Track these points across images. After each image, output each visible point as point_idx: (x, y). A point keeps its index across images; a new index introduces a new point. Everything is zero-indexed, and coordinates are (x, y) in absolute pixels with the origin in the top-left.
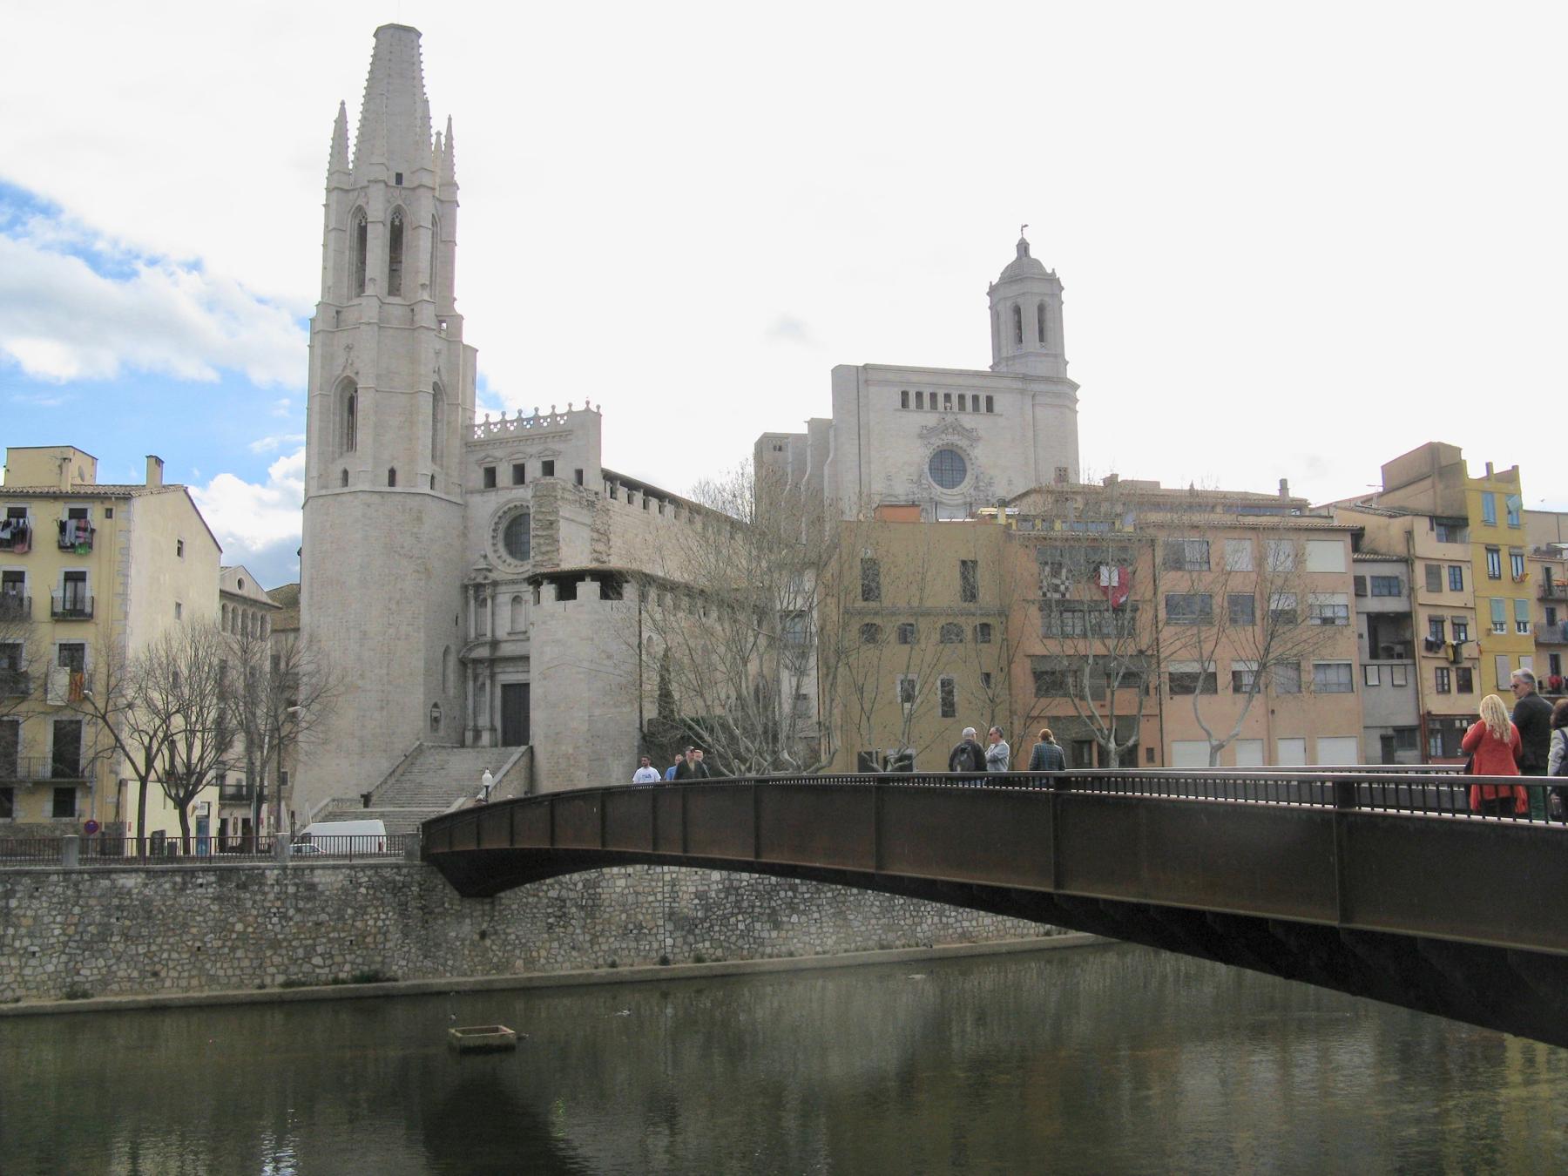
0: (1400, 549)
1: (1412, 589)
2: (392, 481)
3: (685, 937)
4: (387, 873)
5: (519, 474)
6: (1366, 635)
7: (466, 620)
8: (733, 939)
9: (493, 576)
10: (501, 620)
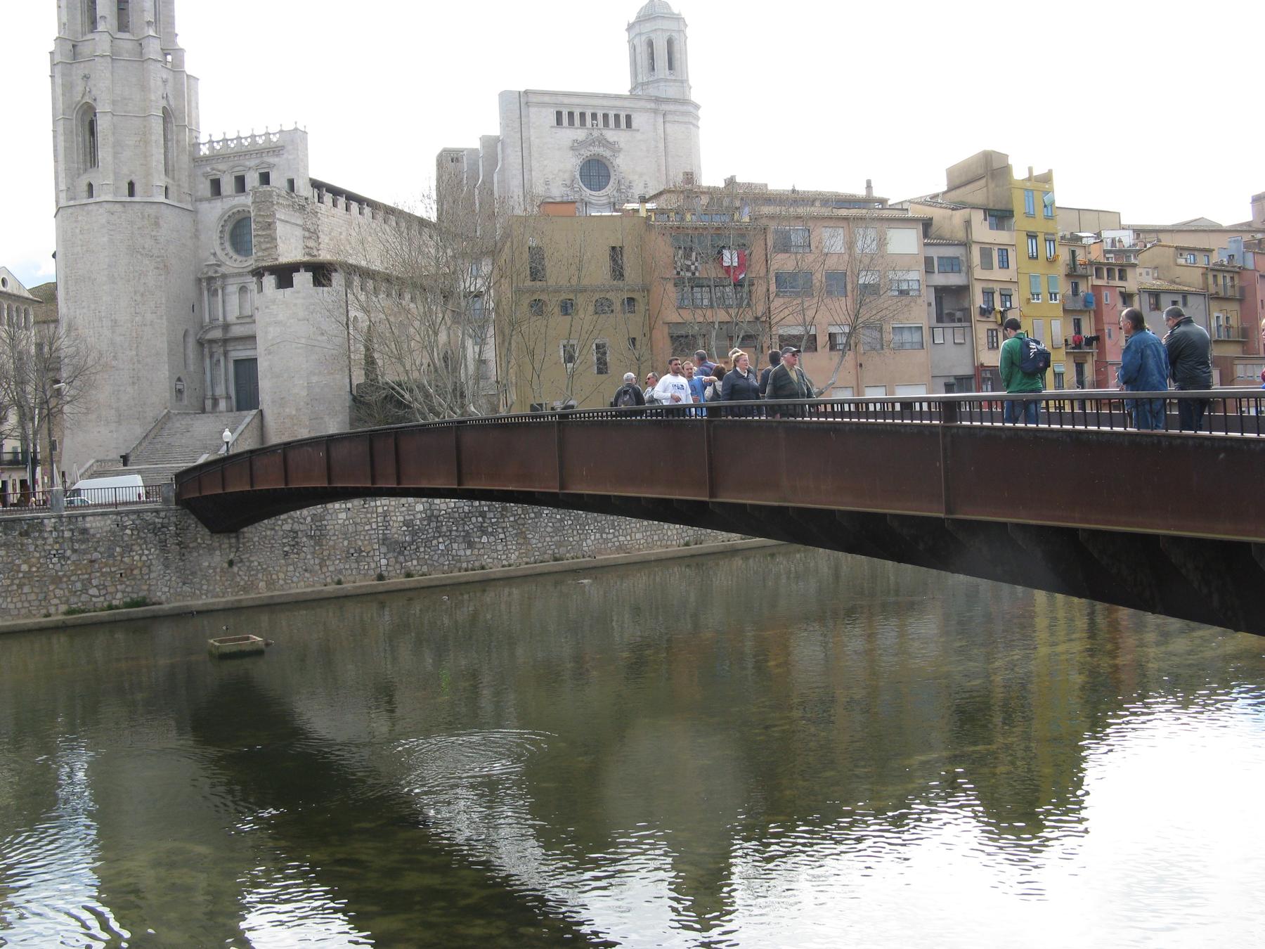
0: (961, 235)
1: (970, 268)
2: (131, 192)
3: (396, 558)
4: (148, 516)
5: (240, 183)
6: (934, 304)
7: (201, 308)
8: (436, 557)
9: (223, 270)
10: (231, 306)
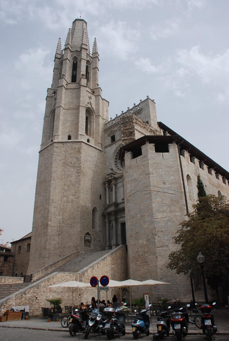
7: (106, 198)
